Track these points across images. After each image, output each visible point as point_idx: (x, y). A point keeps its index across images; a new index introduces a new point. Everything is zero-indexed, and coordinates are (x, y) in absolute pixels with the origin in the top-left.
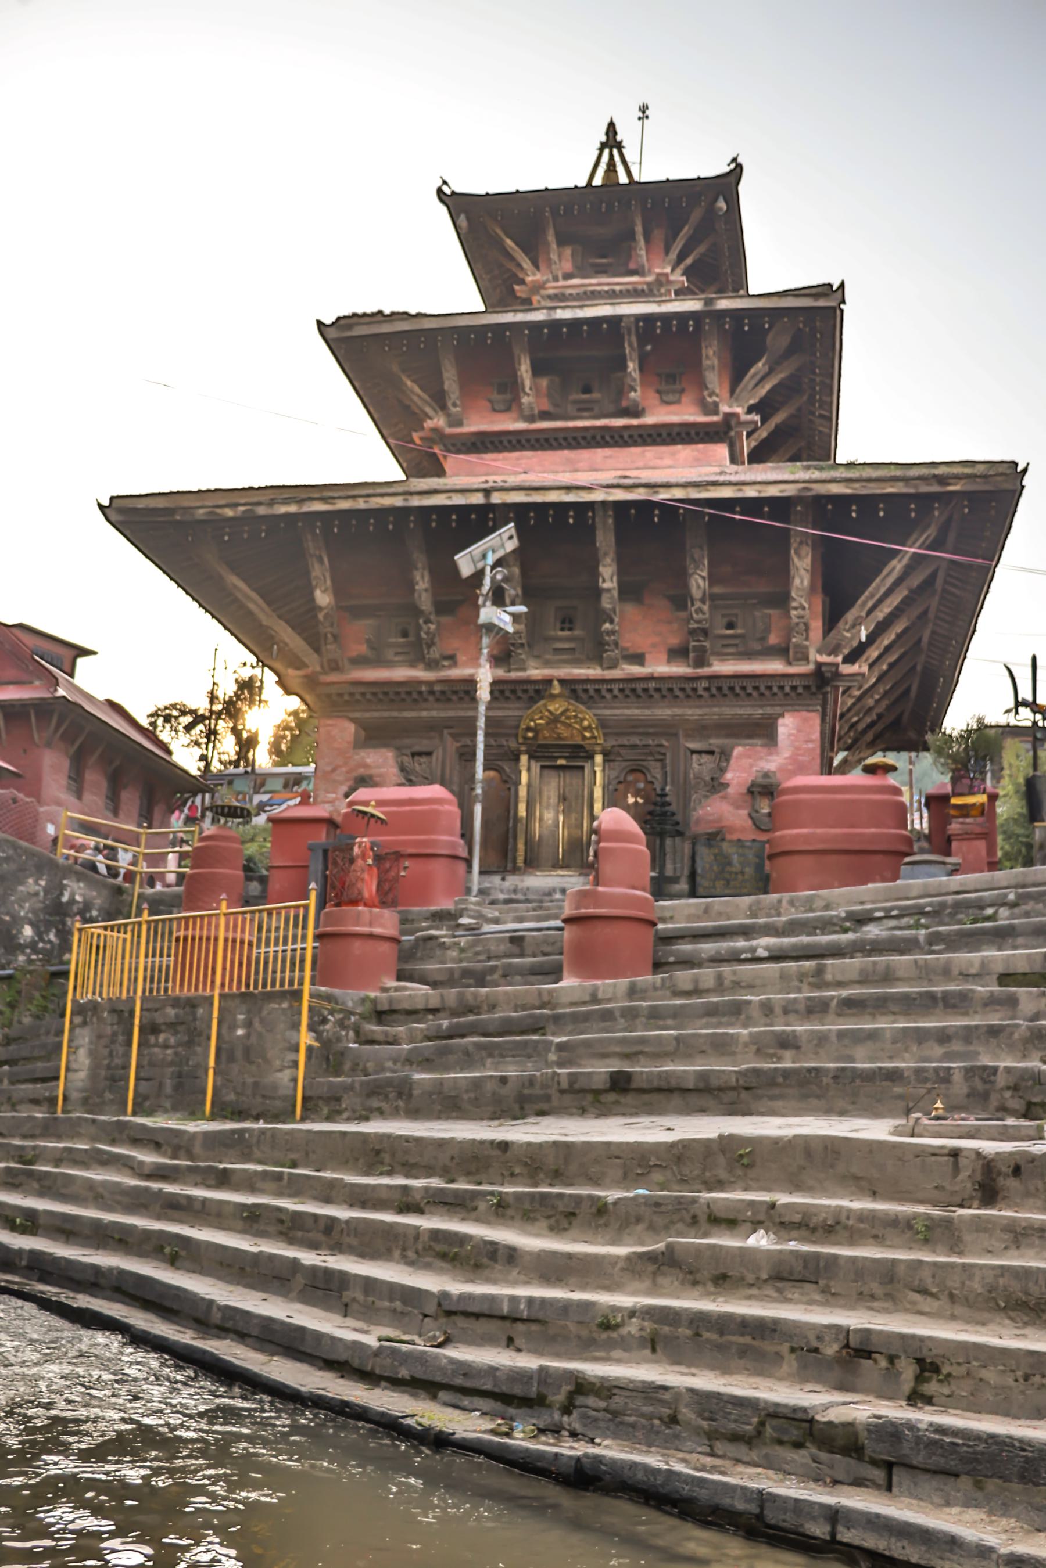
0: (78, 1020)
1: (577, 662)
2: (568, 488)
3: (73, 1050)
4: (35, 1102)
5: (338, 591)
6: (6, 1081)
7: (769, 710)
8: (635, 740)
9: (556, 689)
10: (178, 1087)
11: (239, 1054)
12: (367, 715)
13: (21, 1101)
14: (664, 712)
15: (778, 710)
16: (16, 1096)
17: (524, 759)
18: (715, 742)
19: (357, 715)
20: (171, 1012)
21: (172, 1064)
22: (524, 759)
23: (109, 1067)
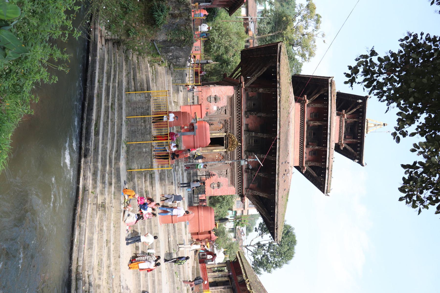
0: (146, 95)
2: (279, 157)
6: (133, 66)
7: (236, 185)
8: (229, 157)
11: (140, 150)
12: (235, 98)
13: (128, 78)
15: (236, 187)
16: (129, 75)
17: (225, 134)
18: (229, 174)
19: (235, 96)
21: (138, 128)
22: (225, 134)
23: (136, 107)
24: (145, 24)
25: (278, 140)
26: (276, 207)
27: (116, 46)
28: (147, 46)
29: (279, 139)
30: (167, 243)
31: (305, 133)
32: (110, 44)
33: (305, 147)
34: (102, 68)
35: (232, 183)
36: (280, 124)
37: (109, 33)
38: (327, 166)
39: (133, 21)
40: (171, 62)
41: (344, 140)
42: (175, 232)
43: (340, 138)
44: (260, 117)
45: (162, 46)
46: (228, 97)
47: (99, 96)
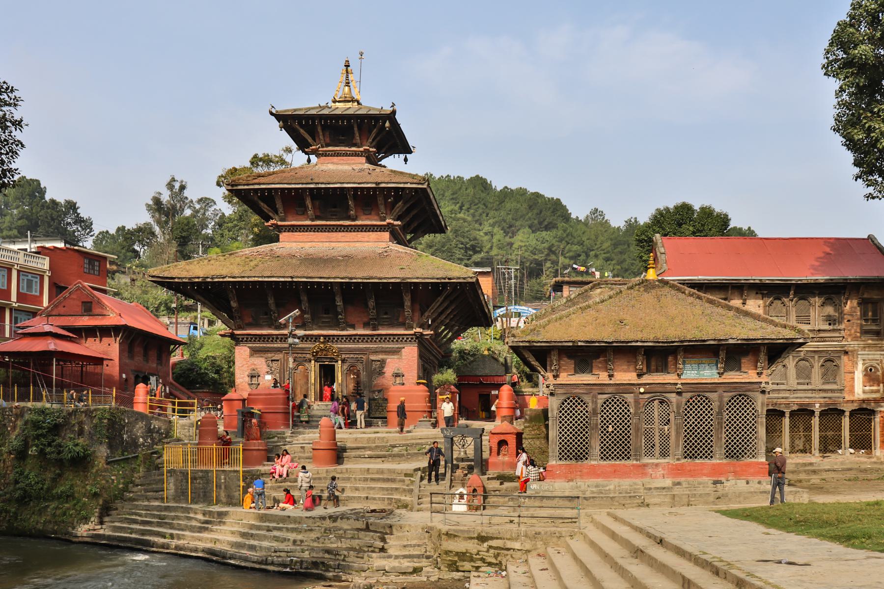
1: (331, 327)
3: (168, 484)
4: (156, 499)
5: (239, 301)
9: (322, 339)
10: (205, 496)
14: (362, 346)
18: (380, 357)
20: (201, 474)
24: (88, 472)
25: (295, 280)
26: (409, 281)
27: (111, 512)
28: (119, 471)
29: (292, 277)
30: (372, 460)
31: (328, 223)
32: (106, 519)
33: (353, 223)
34: (121, 529)
35: (397, 352)
36: (268, 277)
37: (92, 519)
38: (374, 185)
39: (84, 487)
40: (160, 441)
41: (359, 147)
42: (358, 448)
43: (356, 154)
44: (277, 305)
45: (120, 451)
46: (251, 355)
47: (143, 533)
